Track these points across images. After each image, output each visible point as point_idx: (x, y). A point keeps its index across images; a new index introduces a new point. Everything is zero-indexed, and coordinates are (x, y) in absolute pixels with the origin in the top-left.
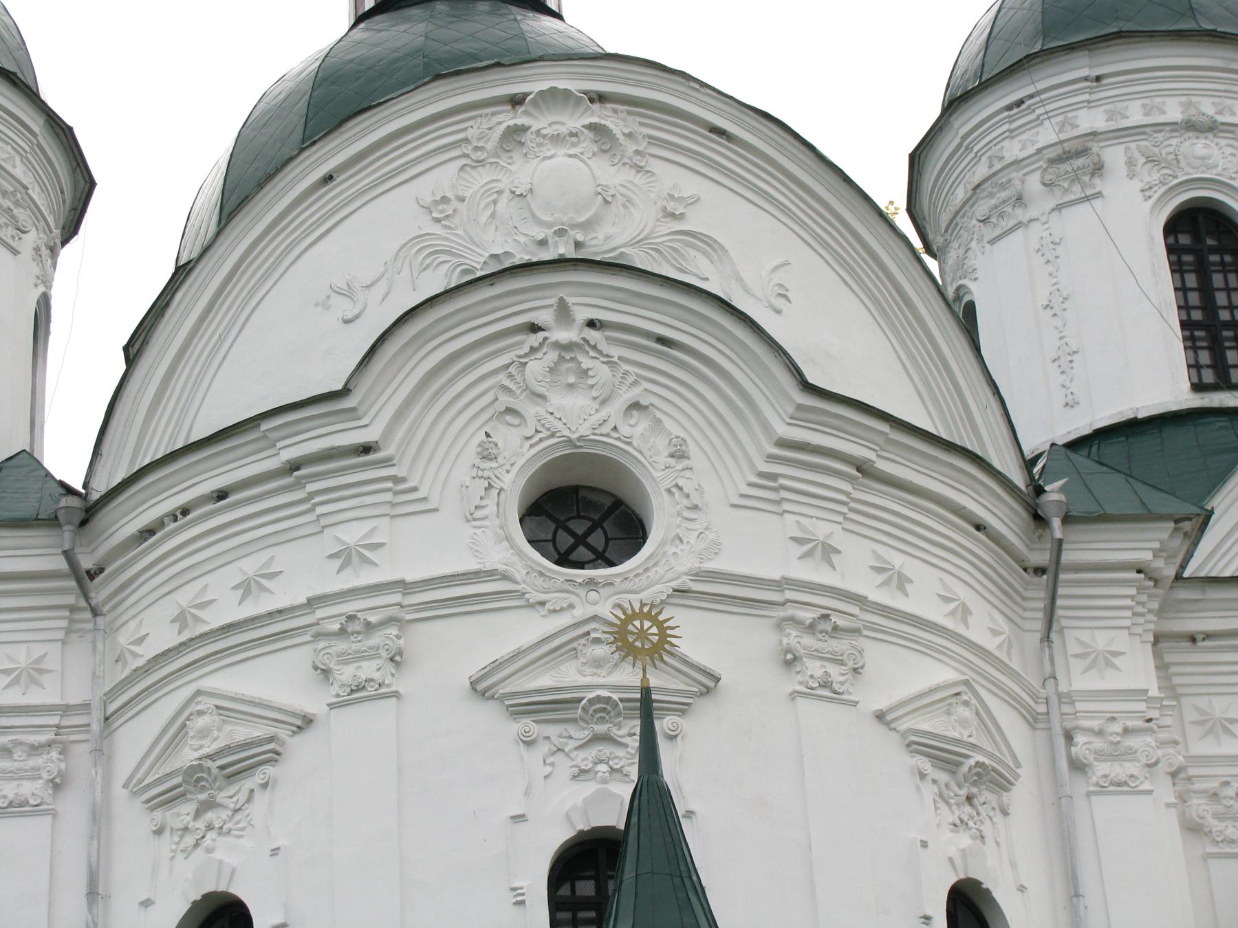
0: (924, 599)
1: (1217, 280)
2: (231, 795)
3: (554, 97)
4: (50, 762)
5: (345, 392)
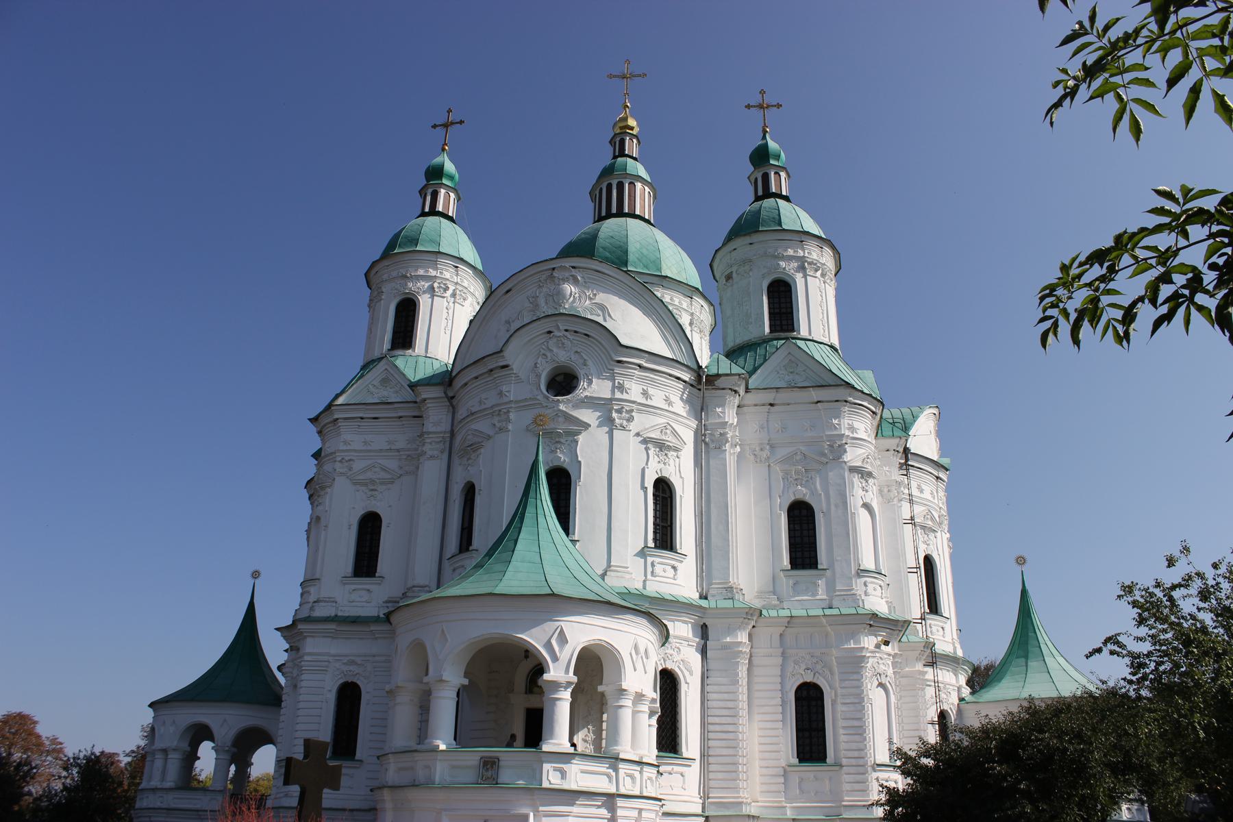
0: (657, 399)
5: (501, 351)
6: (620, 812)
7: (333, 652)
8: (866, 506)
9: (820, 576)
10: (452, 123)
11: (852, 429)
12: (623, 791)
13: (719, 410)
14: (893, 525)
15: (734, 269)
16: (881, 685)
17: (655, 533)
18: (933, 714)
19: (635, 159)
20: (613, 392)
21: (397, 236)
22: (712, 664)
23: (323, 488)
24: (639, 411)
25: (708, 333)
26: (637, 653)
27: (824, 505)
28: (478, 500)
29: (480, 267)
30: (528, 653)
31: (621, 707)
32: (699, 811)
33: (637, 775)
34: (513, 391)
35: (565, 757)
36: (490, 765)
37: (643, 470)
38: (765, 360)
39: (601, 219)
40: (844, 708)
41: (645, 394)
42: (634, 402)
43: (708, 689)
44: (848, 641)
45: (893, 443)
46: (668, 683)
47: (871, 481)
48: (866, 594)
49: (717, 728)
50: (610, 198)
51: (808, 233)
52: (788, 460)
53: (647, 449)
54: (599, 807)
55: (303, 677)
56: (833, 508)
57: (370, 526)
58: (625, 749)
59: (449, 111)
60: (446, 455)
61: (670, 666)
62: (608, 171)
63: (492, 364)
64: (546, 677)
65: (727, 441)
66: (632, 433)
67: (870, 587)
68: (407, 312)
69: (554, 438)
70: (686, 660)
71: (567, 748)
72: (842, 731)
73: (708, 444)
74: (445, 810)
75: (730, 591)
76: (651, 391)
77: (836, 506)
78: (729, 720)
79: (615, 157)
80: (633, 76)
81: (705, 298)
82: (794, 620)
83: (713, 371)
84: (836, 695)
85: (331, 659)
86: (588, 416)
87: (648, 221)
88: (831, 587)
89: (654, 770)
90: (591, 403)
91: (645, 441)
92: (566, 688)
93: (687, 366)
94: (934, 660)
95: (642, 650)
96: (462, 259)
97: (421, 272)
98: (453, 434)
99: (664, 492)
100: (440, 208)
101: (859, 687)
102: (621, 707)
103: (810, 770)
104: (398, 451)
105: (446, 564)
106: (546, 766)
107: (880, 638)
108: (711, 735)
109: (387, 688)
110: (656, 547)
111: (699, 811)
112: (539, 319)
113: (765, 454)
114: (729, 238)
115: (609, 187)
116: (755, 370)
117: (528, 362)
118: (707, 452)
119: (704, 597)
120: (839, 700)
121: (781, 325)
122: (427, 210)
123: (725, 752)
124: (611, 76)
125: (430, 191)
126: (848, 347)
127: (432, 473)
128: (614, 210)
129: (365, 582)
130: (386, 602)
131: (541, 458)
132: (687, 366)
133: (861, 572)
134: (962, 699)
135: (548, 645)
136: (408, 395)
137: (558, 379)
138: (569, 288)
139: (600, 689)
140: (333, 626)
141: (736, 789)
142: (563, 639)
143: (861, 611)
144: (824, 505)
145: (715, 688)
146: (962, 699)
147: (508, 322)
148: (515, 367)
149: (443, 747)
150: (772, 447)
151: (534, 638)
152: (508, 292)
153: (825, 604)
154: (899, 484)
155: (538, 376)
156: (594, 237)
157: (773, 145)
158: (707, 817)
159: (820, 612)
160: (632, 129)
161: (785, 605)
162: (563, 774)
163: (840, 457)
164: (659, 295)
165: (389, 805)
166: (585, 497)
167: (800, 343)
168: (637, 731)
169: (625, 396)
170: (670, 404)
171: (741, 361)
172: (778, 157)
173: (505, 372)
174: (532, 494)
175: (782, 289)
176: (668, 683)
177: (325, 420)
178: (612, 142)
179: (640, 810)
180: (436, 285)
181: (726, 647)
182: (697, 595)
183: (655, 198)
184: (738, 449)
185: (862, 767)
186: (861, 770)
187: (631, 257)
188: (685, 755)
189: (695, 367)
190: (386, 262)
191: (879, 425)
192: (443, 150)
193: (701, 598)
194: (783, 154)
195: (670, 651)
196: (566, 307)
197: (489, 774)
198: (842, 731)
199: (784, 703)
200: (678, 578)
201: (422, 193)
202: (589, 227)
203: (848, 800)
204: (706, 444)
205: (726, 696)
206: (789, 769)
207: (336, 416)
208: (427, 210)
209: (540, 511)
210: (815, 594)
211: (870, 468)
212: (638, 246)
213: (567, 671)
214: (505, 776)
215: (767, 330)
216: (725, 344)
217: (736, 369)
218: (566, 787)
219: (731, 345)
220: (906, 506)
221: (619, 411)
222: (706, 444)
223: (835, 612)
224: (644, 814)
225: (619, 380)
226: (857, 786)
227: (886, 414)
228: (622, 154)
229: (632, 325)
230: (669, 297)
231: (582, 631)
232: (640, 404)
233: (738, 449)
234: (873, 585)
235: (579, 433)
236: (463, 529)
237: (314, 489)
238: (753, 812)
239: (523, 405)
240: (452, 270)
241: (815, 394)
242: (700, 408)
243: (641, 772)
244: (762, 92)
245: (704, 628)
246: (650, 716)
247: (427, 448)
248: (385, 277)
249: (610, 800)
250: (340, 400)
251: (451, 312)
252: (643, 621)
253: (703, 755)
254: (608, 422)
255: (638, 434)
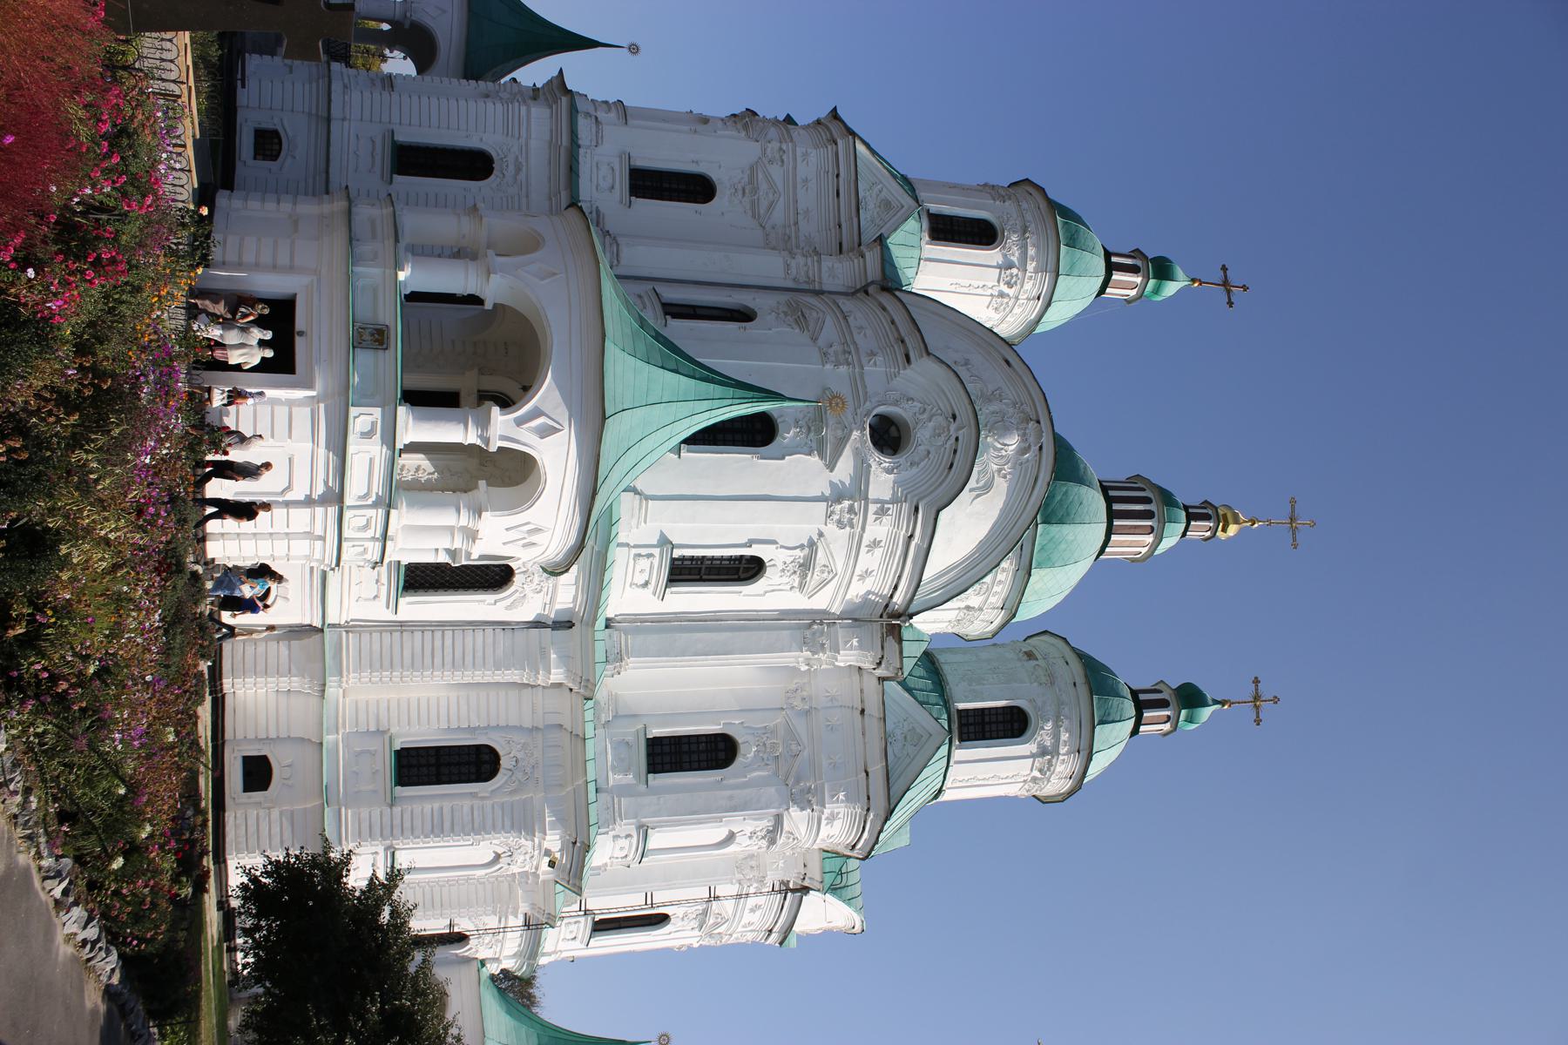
1: (1001, 727)
2: (790, 319)
3: (1040, 434)
4: (802, 278)
5: (929, 354)
6: (319, 510)
7: (533, 144)
8: (731, 837)
9: (637, 776)
10: (1229, 292)
11: (832, 818)
12: (347, 514)
13: (855, 642)
14: (708, 871)
15: (1041, 662)
16: (498, 857)
17: (692, 559)
18: (462, 926)
19: (1184, 534)
20: (876, 501)
21: (1078, 220)
22: (520, 635)
23: (746, 127)
24: (852, 536)
25: (955, 630)
26: (530, 532)
27: (732, 781)
28: (732, 326)
29: (1039, 329)
30: (527, 389)
31: (459, 511)
32: (329, 620)
33: (370, 533)
34: (876, 370)
35: (390, 437)
36: (377, 338)
37: (774, 542)
38: (921, 703)
39: (1105, 490)
40: (466, 809)
41: (875, 544)
42: (863, 529)
43: (489, 630)
44: (554, 813)
45: (815, 872)
46: (494, 577)
47: (764, 843)
48: (616, 837)
49: (438, 643)
50: (1131, 501)
51: (1089, 759)
52: (791, 733)
53: (802, 547)
54: (326, 483)
55: (499, 105)
56: (728, 793)
57: (697, 188)
58: (402, 517)
59: (1245, 288)
60: (790, 284)
61: (517, 579)
62: (1167, 499)
63: (912, 343)
64: (496, 410)
65: (814, 653)
66: (823, 528)
67: (624, 842)
68: (979, 234)
69: (814, 424)
70: (524, 601)
71: (403, 439)
72: (436, 806)
73: (810, 627)
74: (319, 280)
75: (616, 658)
76: (878, 552)
77: (731, 798)
78: (448, 659)
79: (1186, 508)
80: (1294, 531)
81: (1003, 626)
82: (580, 742)
83: (906, 634)
84: (483, 798)
85: (523, 141)
86: (845, 469)
87: (1102, 551)
88: (623, 790)
89: (376, 557)
90: (862, 472)
91: (812, 544)
92: (481, 437)
93: (911, 600)
94: (533, 927)
95: (534, 539)
96: (1049, 304)
97: (1031, 251)
98: (819, 293)
99: (746, 569)
100: (1117, 276)
101: (494, 828)
102: (459, 511)
103: (386, 766)
104: (796, 223)
105: (649, 286)
106: (377, 412)
107: (558, 855)
108: (428, 635)
109: (481, 205)
110: (673, 560)
111: (329, 620)
112: (972, 402)
113: (800, 705)
114: (1081, 656)
115: (1147, 501)
116: (909, 690)
117: (914, 389)
118: (799, 627)
119: (609, 624)
120: (477, 803)
121: (967, 725)
122: (1114, 259)
123: (407, 653)
124: (1293, 502)
125: (1139, 263)
126: (937, 811)
127: (768, 266)
128: (1116, 507)
129: (622, 182)
130: (598, 211)
131: (786, 404)
132: (911, 600)
133: (644, 831)
134: (483, 963)
135: (537, 413)
136: (869, 234)
137: (893, 429)
138: (1013, 442)
139: (482, 483)
140: (565, 141)
141: (359, 668)
142: (545, 432)
143: (593, 830)
144: (732, 781)
145: (490, 640)
146: (483, 963)
147: (967, 363)
148: (908, 371)
149: (402, 276)
150: (807, 713)
151: (547, 394)
152: (1007, 362)
153: (601, 784)
154: (762, 881)
155: (896, 403)
156: (1081, 480)
157: (1205, 713)
158: (322, 630)
159: (591, 776)
160: (1224, 530)
161: (600, 731)
162: (367, 435)
163: (795, 802)
164: (1004, 565)
165: (326, 208)
166: (736, 467)
167: (944, 750)
168: (428, 535)
169: (871, 517)
170: (862, 577)
171: (920, 672)
172: (1190, 720)
173: (901, 359)
174: (740, 393)
175: (1016, 726)
176: (494, 577)
177: (835, 128)
178: (1206, 504)
179: (323, 538)
180: (1015, 271)
181: (544, 654)
182: (611, 615)
183: (1133, 561)
184: (804, 668)
185: (390, 833)
186: (387, 831)
187: (1054, 529)
188: (401, 600)
189: (911, 610)
190: (1043, 205)
191: (838, 854)
192: (1194, 280)
193: (608, 620)
194: (1193, 727)
195: (536, 579)
196: (987, 439)
197: (367, 337)
198: (436, 806)
199: (471, 730)
200: (633, 590)
201: (1136, 253)
202: (1094, 475)
203: (348, 815)
204: (810, 626)
205: (479, 654)
206: (387, 737)
207: (840, 142)
208: (1114, 259)
209: (717, 403)
210: (614, 768)
211: (781, 841)
212: (1070, 538)
213: (503, 438)
214: (365, 357)
215: (961, 706)
216: (943, 651)
217: (909, 664)
218: (351, 438)
219: (941, 658)
220: (733, 889)
221: (851, 510)
222: (810, 626)
223: (592, 796)
224: (319, 543)
225: (893, 509)
226: (365, 826)
227: (853, 864)
228: (1190, 517)
229: (965, 526)
230: (1001, 580)
231: (557, 457)
232: (861, 537)
233: (804, 668)
234: (628, 846)
235: (822, 456)
236: (694, 307)
237: (747, 119)
238: (332, 691)
239: (857, 383)
240: (1035, 293)
241: (877, 769)
242: (856, 617)
243: (374, 539)
244: (1276, 700)
245: (569, 625)
246: (448, 551)
247: (800, 260)
248: (1024, 205)
249: (335, 497)
250: (860, 148)
251: (979, 291)
252: (572, 540)
253: (402, 625)
254: (838, 495)
255: (821, 535)
